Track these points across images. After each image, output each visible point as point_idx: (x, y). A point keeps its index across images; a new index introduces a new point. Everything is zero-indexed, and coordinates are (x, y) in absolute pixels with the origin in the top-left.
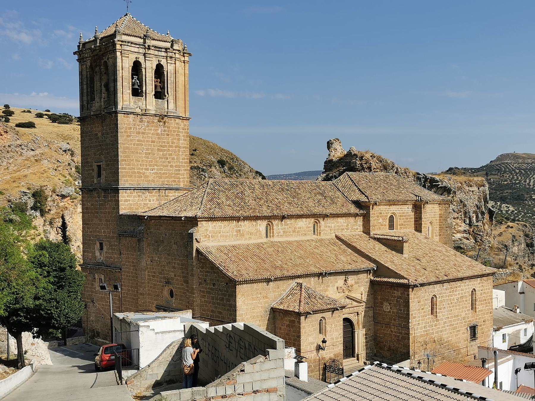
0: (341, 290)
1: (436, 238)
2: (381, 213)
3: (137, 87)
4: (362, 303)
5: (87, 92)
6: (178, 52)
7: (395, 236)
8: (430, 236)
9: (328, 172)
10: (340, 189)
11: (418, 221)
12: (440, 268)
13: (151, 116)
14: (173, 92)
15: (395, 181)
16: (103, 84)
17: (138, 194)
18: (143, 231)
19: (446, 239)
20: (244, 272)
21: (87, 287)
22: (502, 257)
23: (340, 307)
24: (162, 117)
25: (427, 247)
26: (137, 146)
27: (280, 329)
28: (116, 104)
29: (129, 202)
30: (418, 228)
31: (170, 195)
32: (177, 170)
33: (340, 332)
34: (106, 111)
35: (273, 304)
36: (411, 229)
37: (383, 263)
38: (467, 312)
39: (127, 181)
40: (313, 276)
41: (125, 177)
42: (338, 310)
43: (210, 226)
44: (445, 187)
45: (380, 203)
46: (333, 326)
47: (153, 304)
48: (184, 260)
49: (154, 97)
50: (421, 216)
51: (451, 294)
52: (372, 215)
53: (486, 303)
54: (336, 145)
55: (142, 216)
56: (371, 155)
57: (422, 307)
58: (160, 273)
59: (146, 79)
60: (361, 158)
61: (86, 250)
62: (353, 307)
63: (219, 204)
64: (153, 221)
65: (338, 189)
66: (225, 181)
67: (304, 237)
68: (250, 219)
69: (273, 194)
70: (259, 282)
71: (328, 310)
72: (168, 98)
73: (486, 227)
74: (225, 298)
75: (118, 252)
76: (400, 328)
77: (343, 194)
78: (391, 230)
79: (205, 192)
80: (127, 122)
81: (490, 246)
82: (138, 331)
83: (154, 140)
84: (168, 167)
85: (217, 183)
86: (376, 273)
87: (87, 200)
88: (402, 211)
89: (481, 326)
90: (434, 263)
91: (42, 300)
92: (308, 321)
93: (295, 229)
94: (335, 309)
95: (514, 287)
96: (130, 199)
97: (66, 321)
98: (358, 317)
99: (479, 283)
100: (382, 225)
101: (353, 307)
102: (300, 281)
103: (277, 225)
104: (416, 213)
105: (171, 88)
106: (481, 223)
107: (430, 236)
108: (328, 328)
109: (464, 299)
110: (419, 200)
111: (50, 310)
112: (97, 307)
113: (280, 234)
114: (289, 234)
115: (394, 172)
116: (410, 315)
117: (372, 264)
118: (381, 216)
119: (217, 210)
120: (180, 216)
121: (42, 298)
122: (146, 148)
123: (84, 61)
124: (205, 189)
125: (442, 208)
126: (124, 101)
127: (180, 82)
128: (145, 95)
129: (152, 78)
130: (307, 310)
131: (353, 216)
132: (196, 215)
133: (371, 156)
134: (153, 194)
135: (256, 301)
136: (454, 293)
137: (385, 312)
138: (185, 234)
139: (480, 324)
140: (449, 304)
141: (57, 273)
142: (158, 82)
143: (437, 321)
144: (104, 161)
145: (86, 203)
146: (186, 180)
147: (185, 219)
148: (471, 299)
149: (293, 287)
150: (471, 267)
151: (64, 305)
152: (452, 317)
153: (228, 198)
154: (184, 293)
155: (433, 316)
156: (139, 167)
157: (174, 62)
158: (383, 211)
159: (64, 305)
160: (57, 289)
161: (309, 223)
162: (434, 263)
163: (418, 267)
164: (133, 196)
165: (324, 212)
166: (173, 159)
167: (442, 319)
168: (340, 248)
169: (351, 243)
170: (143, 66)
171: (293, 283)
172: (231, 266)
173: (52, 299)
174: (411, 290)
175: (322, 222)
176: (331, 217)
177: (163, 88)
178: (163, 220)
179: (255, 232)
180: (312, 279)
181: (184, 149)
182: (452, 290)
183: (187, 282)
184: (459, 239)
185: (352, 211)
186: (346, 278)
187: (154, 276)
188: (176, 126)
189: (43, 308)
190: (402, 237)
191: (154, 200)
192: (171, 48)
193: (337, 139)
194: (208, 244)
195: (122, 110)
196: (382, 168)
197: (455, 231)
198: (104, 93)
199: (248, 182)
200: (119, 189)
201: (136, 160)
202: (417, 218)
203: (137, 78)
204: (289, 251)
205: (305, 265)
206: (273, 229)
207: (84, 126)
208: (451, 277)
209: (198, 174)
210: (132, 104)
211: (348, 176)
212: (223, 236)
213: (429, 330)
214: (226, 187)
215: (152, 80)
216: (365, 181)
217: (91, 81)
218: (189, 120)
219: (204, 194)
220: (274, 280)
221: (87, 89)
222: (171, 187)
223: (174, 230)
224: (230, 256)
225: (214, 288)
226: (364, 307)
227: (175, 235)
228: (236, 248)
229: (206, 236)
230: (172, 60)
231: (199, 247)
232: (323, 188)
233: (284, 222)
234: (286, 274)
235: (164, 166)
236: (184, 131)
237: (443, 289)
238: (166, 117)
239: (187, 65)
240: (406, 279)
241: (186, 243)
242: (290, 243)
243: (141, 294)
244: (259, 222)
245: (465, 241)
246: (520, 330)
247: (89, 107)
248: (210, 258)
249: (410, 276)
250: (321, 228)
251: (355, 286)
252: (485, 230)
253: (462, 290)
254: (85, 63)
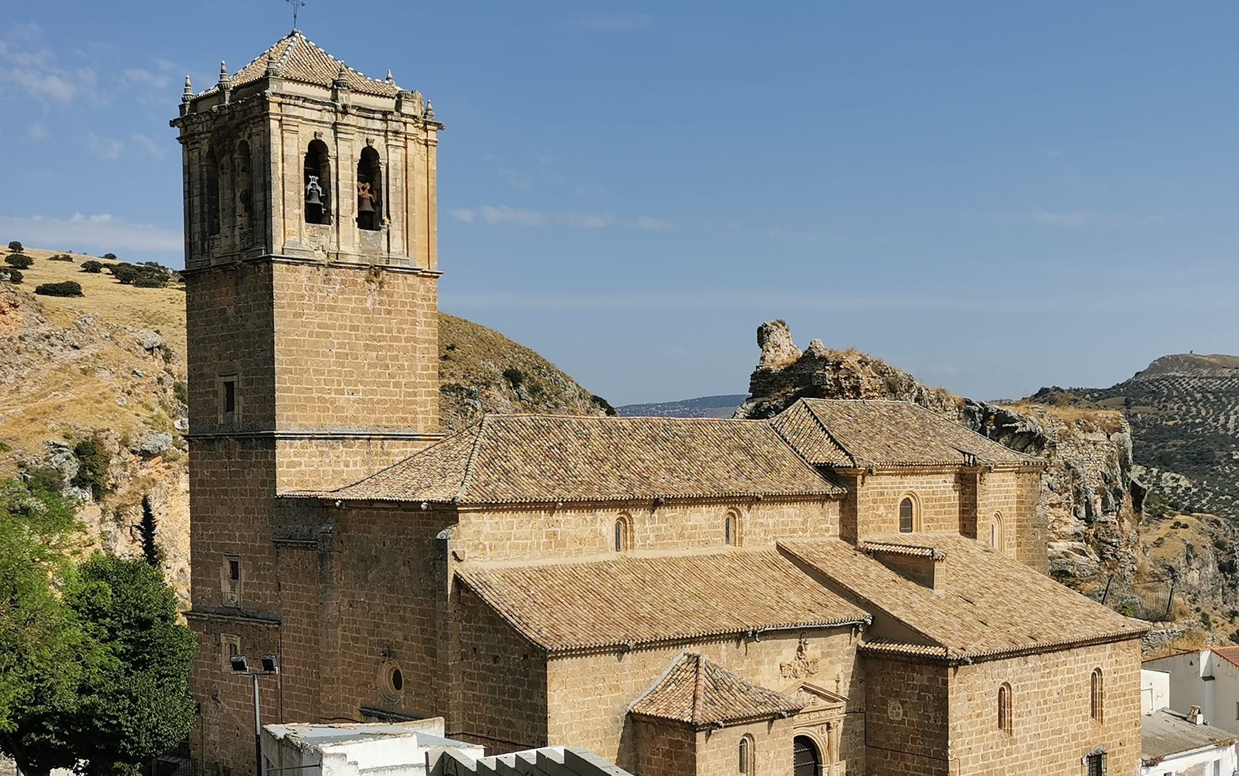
0: (790, 672)
1: (1011, 552)
2: (882, 494)
3: (317, 201)
4: (838, 701)
7: (914, 547)
8: (996, 546)
9: (760, 400)
10: (788, 438)
11: (968, 510)
12: (1020, 620)
13: (350, 268)
14: (400, 213)
15: (915, 418)
17: (320, 449)
18: (330, 535)
19: (1034, 553)
20: (564, 630)
21: (202, 665)
22: (1163, 595)
23: (787, 712)
24: (375, 271)
25: (989, 572)
26: (316, 337)
27: (649, 761)
28: (268, 241)
29: (298, 469)
30: (968, 527)
31: (393, 450)
32: (409, 394)
33: (788, 769)
34: (244, 257)
35: (632, 704)
36: (952, 530)
37: (888, 610)
38: (1080, 722)
39: (295, 418)
40: (724, 639)
41: (290, 411)
42: (783, 717)
43: (487, 522)
44: (1031, 433)
45: (881, 470)
46: (772, 755)
47: (354, 702)
48: (426, 601)
49: (356, 224)
50: (976, 500)
51: (1046, 679)
52: (862, 499)
53: (1126, 702)
54: (778, 336)
55: (328, 500)
56: (860, 358)
57: (978, 711)
58: (371, 633)
59: (339, 182)
60: (837, 366)
61: (200, 578)
62: (818, 711)
63: (506, 472)
64: (354, 512)
65: (782, 437)
66: (520, 418)
67: (704, 549)
68: (579, 508)
69: (632, 450)
70: (601, 653)
71: (760, 718)
72: (388, 226)
73: (1127, 525)
74: (521, 689)
75: (274, 584)
76: (926, 759)
77: (795, 450)
78: (905, 531)
79: (474, 444)
80: (294, 283)
81: (1136, 569)
82: (320, 766)
83: (357, 324)
84: (389, 387)
85: (502, 423)
86: (870, 632)
87: (201, 464)
88: (930, 488)
89: (1113, 754)
90: (1006, 608)
91: (98, 694)
92: (713, 743)
93: (682, 530)
94: (777, 716)
95: (1191, 664)
96: (302, 460)
97: (153, 742)
98: (828, 733)
99: (1110, 656)
100: (884, 521)
101: (818, 711)
102: (694, 649)
103: (643, 521)
104: (962, 493)
105: (396, 204)
106: (1114, 517)
107: (996, 546)
108: (760, 760)
109: (1075, 693)
110: (971, 462)
111: (116, 718)
112: (225, 711)
113: (648, 542)
114: (670, 541)
115: (913, 398)
116: (950, 729)
117: (860, 610)
118: (881, 501)
119: (503, 485)
120: (416, 499)
121: (97, 690)
122: (338, 343)
124: (475, 438)
125: (1024, 481)
126: (287, 233)
127: (418, 190)
128: (335, 220)
129: (353, 181)
130: (712, 717)
131: (817, 500)
132: (454, 499)
133: (860, 362)
134: (355, 449)
135: (594, 698)
136: (1052, 678)
137: (892, 722)
138: (429, 542)
139: (1111, 750)
140: (1039, 704)
141: (132, 633)
142: (366, 191)
143: (1013, 742)
144: (241, 374)
145: (199, 470)
146: (432, 416)
147: (428, 506)
148: (1090, 693)
149: (679, 664)
150: (1090, 619)
151: (149, 707)
152: (1046, 734)
153: (527, 459)
154: (426, 679)
155: (1002, 731)
156: (323, 386)
157: (402, 144)
158: (887, 488)
159: (149, 707)
160: (132, 668)
161: (716, 517)
162: (1006, 608)
163: (969, 618)
164: (307, 455)
165: (751, 491)
166: (401, 367)
167: (1024, 739)
168: (787, 575)
169: (812, 563)
171: (678, 656)
172: (536, 616)
173: (121, 692)
174: (951, 670)
175: (746, 515)
176: (767, 503)
177: (377, 204)
178: (378, 509)
179: (590, 536)
180: (723, 646)
181: (427, 345)
182: (1047, 670)
183: (433, 653)
184: (1063, 553)
185: (816, 489)
186: (800, 643)
187: (355, 640)
188: (407, 291)
189: (99, 712)
190: (930, 549)
191: (356, 464)
192: (397, 111)
193: (780, 322)
194: (481, 565)
195: (283, 254)
196: (884, 390)
197: (1053, 536)
199: (573, 421)
200: (275, 439)
201: (316, 371)
202: (965, 505)
203: (318, 181)
204: (670, 581)
205: (707, 614)
206: (632, 530)
207: (194, 291)
208: (1043, 641)
209: (458, 403)
210: (305, 240)
211: (806, 406)
212: (517, 547)
213: (994, 764)
214: (523, 432)
215: (353, 185)
216: (844, 419)
217: (212, 188)
218: (437, 277)
219: (473, 450)
220: (634, 649)
222: (396, 433)
223: (403, 533)
224: (532, 592)
225: (495, 666)
226: (843, 710)
227: (405, 545)
228: (545, 574)
229: (476, 547)
230: (399, 139)
231: (460, 573)
232: (747, 436)
233: (659, 513)
234: (663, 634)
235: (379, 385)
236: (425, 303)
237: (1027, 669)
238: (385, 272)
239: (433, 150)
240: (940, 645)
241: (431, 563)
242: (671, 562)
243: (326, 681)
244: (600, 514)
245: (1077, 558)
246: (1204, 764)
247: (206, 247)
248: (487, 596)
249: (950, 638)
250: (744, 528)
251: (823, 663)
252: (1123, 532)
253: (1069, 671)
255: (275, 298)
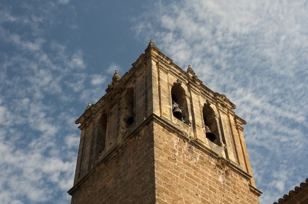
5: (91, 150)
6: (231, 106)
13: (205, 152)
16: (122, 117)
80: (168, 139)
105: (228, 138)
123: (91, 119)
170: (187, 93)
188: (243, 186)
198: (123, 128)
221: (92, 147)
254: (93, 119)
255: (154, 140)
